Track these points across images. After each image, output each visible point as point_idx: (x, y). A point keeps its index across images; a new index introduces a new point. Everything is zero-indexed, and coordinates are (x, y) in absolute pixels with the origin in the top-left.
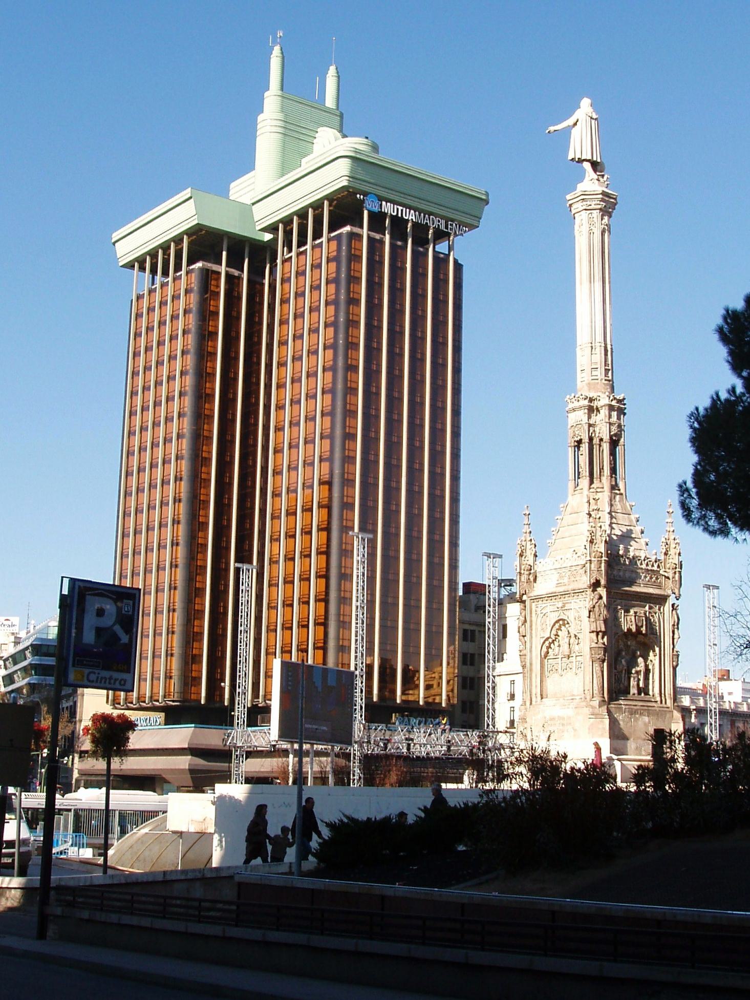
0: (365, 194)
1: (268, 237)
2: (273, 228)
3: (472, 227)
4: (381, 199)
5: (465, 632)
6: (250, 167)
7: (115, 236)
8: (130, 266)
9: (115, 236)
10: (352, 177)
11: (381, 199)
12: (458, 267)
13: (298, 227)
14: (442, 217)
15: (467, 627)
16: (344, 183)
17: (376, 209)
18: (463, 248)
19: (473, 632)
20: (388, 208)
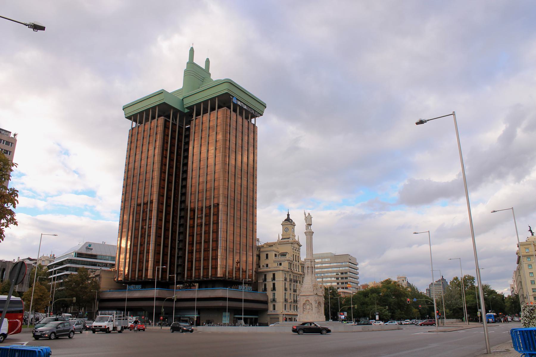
0: (233, 97)
1: (186, 111)
2: (191, 108)
3: (261, 115)
4: (237, 99)
11: (237, 99)
17: (236, 102)
18: (258, 122)
20: (239, 103)
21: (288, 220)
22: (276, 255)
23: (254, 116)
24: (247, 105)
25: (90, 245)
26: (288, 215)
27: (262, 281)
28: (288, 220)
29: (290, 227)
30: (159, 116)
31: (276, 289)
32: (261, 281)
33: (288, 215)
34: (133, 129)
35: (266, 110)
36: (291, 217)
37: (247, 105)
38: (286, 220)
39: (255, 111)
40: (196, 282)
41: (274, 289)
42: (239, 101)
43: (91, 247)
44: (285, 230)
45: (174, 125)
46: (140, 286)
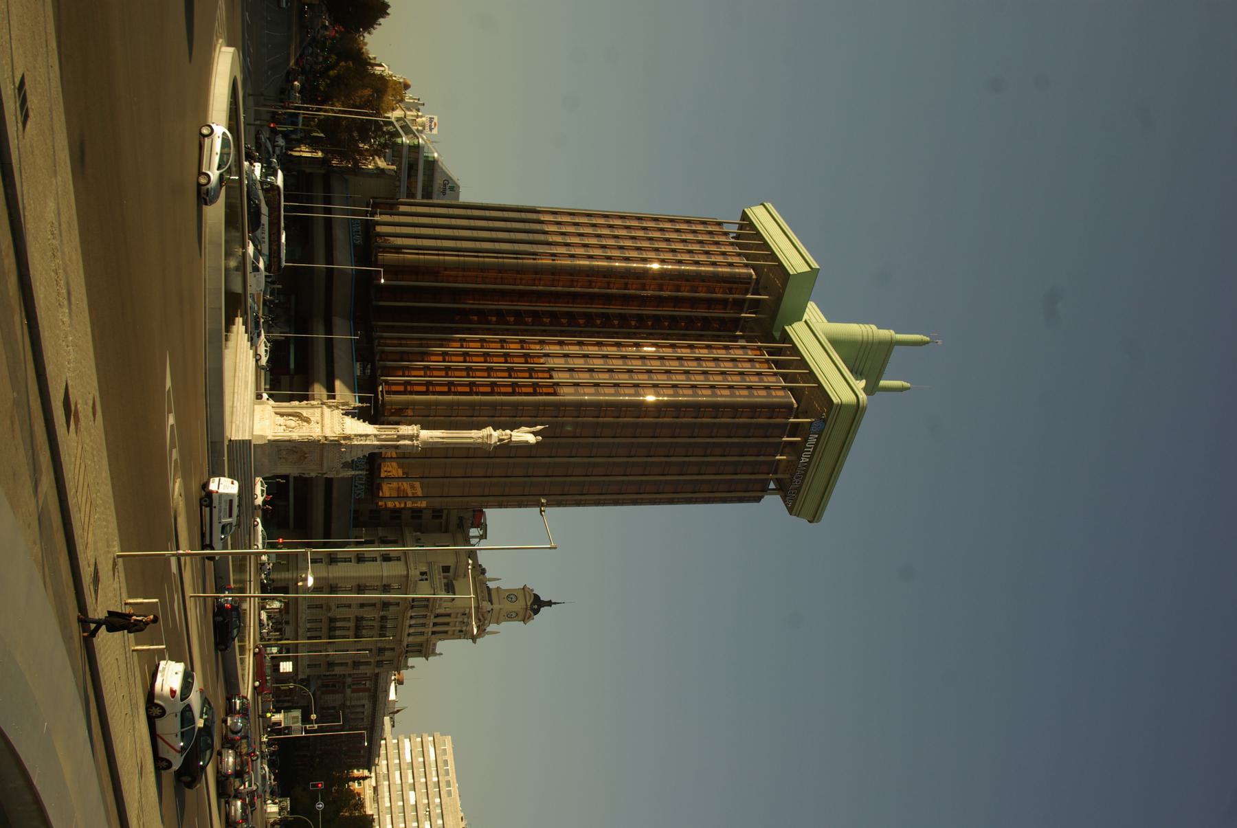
1: (777, 335)
2: (786, 338)
3: (791, 510)
4: (820, 434)
5: (441, 511)
6: (829, 320)
7: (769, 205)
8: (745, 216)
9: (769, 205)
10: (841, 406)
12: (758, 499)
13: (788, 359)
14: (801, 486)
15: (445, 512)
16: (836, 400)
18: (773, 503)
19: (441, 517)
20: (812, 439)
21: (538, 604)
22: (446, 569)
23: (784, 490)
24: (809, 463)
25: (452, 189)
26: (549, 603)
27: (380, 534)
28: (538, 604)
29: (519, 605)
30: (753, 267)
31: (361, 565)
32: (381, 532)
33: (549, 603)
34: (719, 224)
35: (802, 522)
36: (544, 610)
37: (809, 463)
38: (536, 597)
39: (799, 489)
40: (373, 370)
41: (360, 558)
42: (818, 439)
43: (448, 192)
44: (511, 596)
45: (739, 305)
46: (359, 241)
